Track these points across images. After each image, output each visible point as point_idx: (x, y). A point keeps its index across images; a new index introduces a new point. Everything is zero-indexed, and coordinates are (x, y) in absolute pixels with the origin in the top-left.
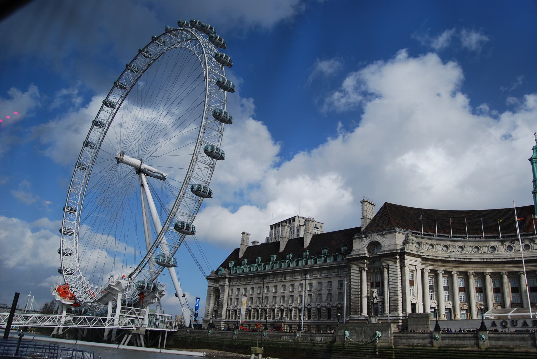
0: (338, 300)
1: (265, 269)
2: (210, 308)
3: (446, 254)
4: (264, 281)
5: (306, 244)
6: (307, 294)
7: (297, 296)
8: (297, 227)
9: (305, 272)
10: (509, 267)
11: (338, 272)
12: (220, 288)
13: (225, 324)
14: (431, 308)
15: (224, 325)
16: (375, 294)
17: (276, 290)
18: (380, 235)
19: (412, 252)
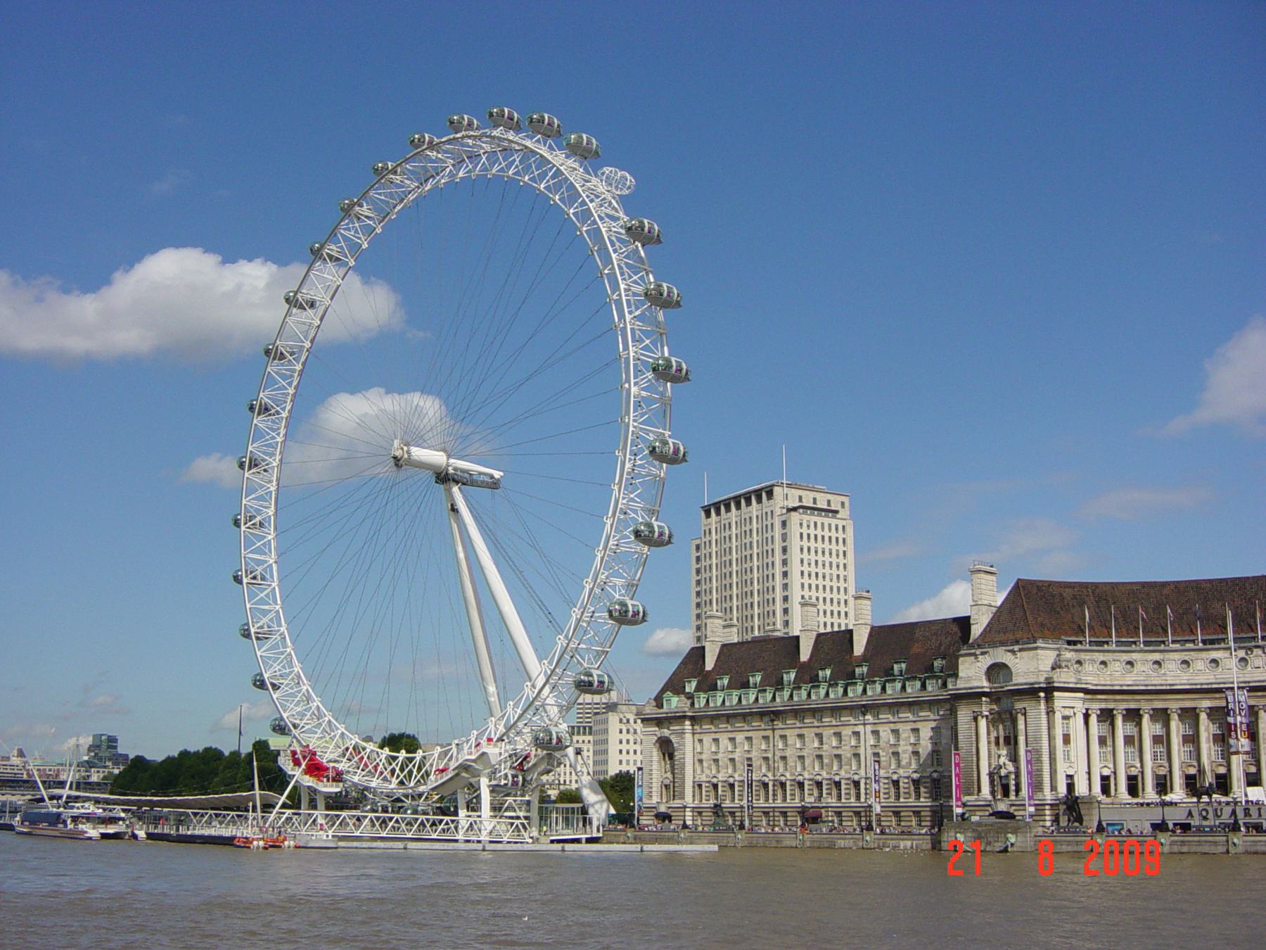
0: (933, 764)
4: (773, 725)
5: (859, 648)
6: (870, 751)
7: (849, 755)
8: (782, 515)
9: (864, 709)
12: (674, 739)
13: (693, 812)
15: (691, 814)
18: (1009, 651)
19: (1066, 685)
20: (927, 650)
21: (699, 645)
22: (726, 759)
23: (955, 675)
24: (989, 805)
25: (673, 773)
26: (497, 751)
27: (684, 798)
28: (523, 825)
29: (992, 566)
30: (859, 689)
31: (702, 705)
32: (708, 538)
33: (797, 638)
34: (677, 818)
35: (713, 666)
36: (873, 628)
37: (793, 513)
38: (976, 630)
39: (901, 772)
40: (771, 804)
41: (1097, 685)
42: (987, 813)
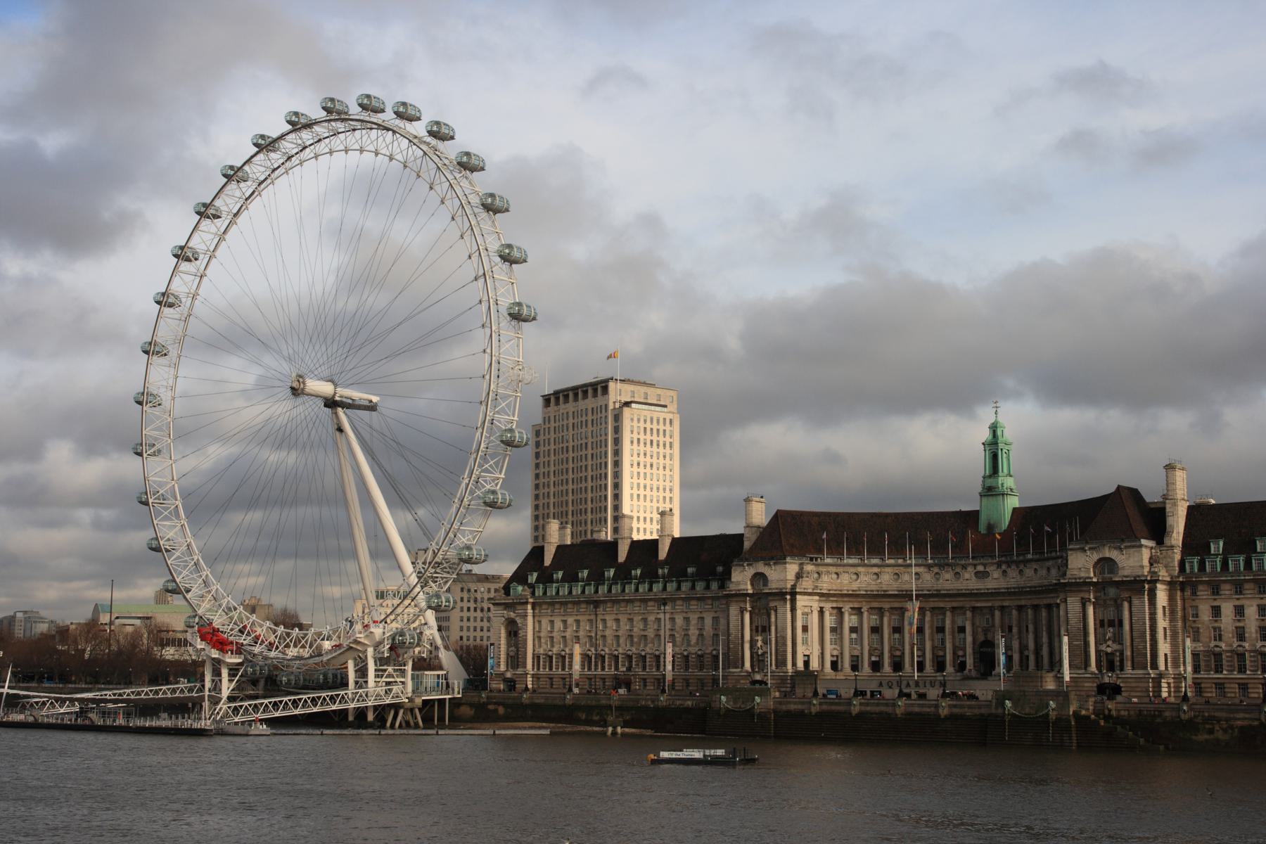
1: (596, 592)
2: (502, 653)
3: (855, 586)
5: (663, 553)
6: (668, 633)
7: (652, 636)
8: (615, 409)
9: (664, 602)
10: (933, 601)
11: (712, 605)
12: (519, 620)
14: (832, 656)
16: (760, 643)
17: (618, 626)
18: (766, 564)
19: (806, 591)
21: (537, 544)
22: (558, 637)
23: (730, 578)
24: (749, 676)
27: (525, 667)
29: (762, 497)
30: (661, 585)
35: (550, 563)
37: (626, 410)
38: (747, 545)
41: (830, 590)
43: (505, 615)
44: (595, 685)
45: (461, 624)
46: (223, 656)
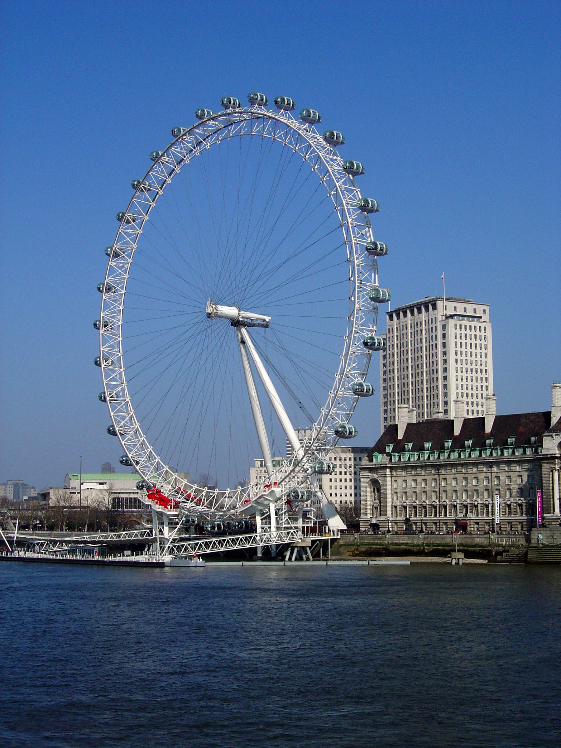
5: (488, 428)
8: (442, 321)
13: (392, 522)
15: (391, 524)
20: (527, 430)
22: (411, 492)
25: (380, 501)
26: (280, 489)
28: (294, 532)
30: (488, 452)
31: (397, 461)
32: (391, 335)
33: (453, 420)
34: (382, 526)
36: (496, 416)
39: (512, 499)
40: (438, 518)
42: (558, 523)
43: (369, 476)
44: (440, 527)
45: (331, 484)
46: (164, 510)
